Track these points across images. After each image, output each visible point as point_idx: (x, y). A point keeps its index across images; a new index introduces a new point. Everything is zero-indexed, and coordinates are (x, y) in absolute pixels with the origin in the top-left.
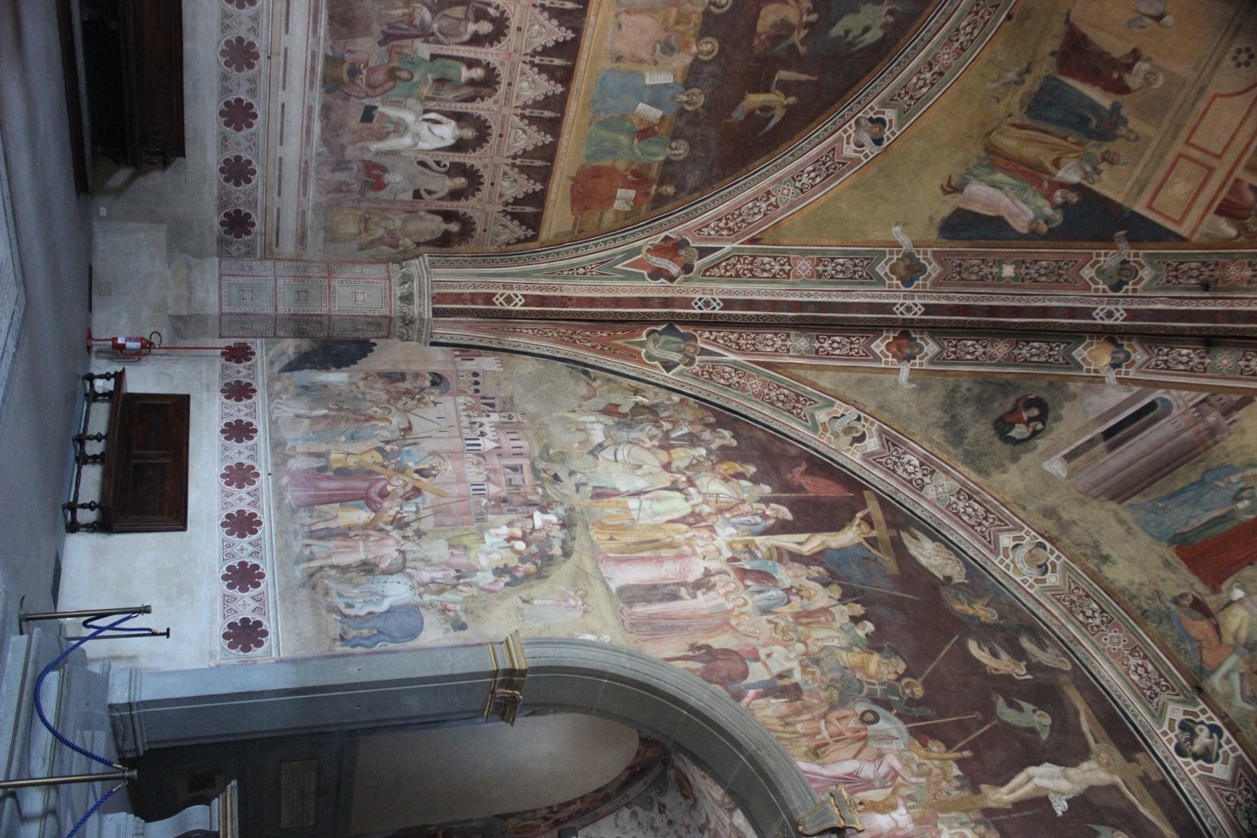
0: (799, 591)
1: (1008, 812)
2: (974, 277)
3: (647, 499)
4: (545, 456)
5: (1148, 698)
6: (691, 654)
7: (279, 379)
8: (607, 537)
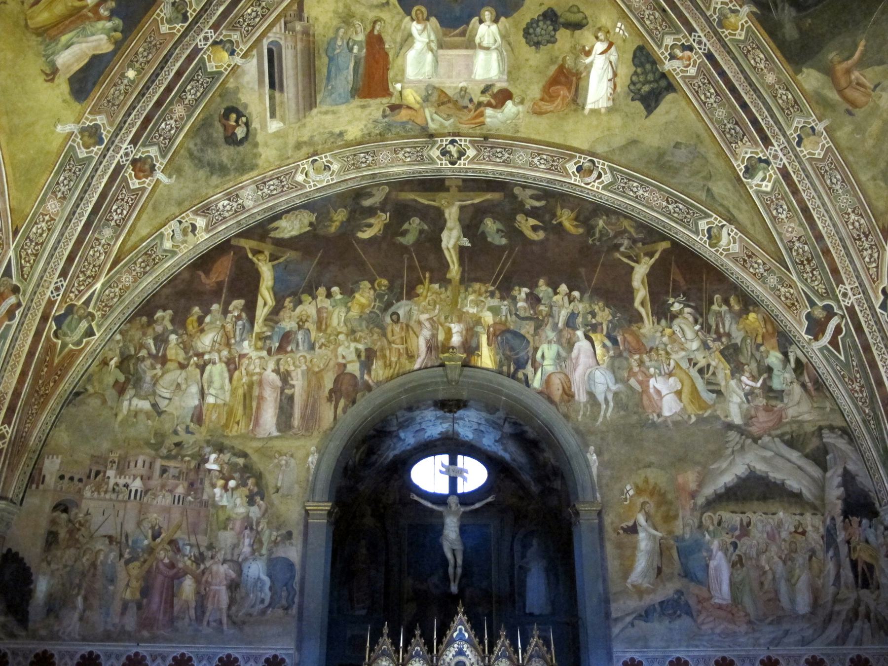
0: (301, 320)
1: (463, 272)
2: (122, 98)
5: (421, 160)
8: (236, 426)
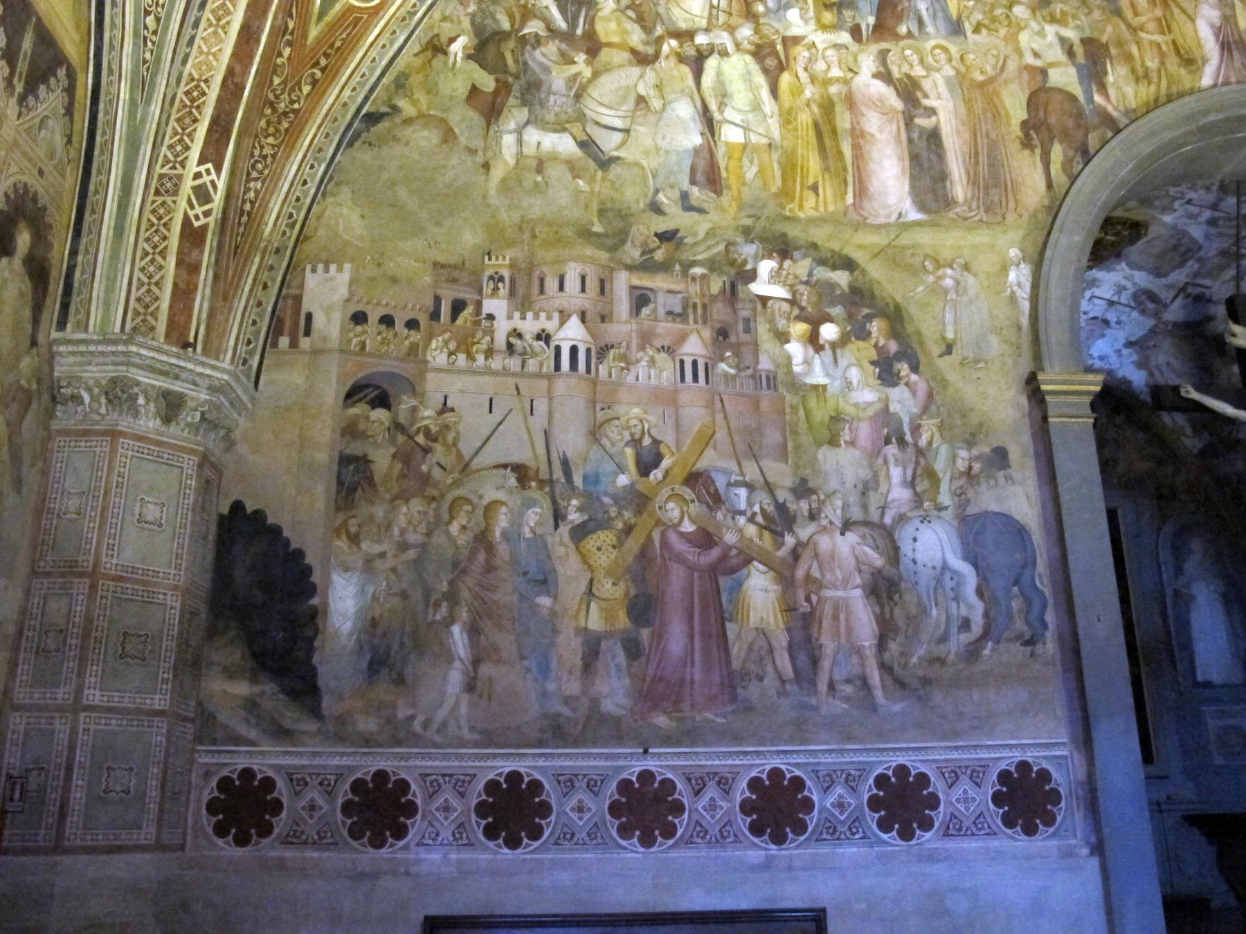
3: (721, 110)
6: (1038, 151)
7: (341, 720)
8: (810, 196)
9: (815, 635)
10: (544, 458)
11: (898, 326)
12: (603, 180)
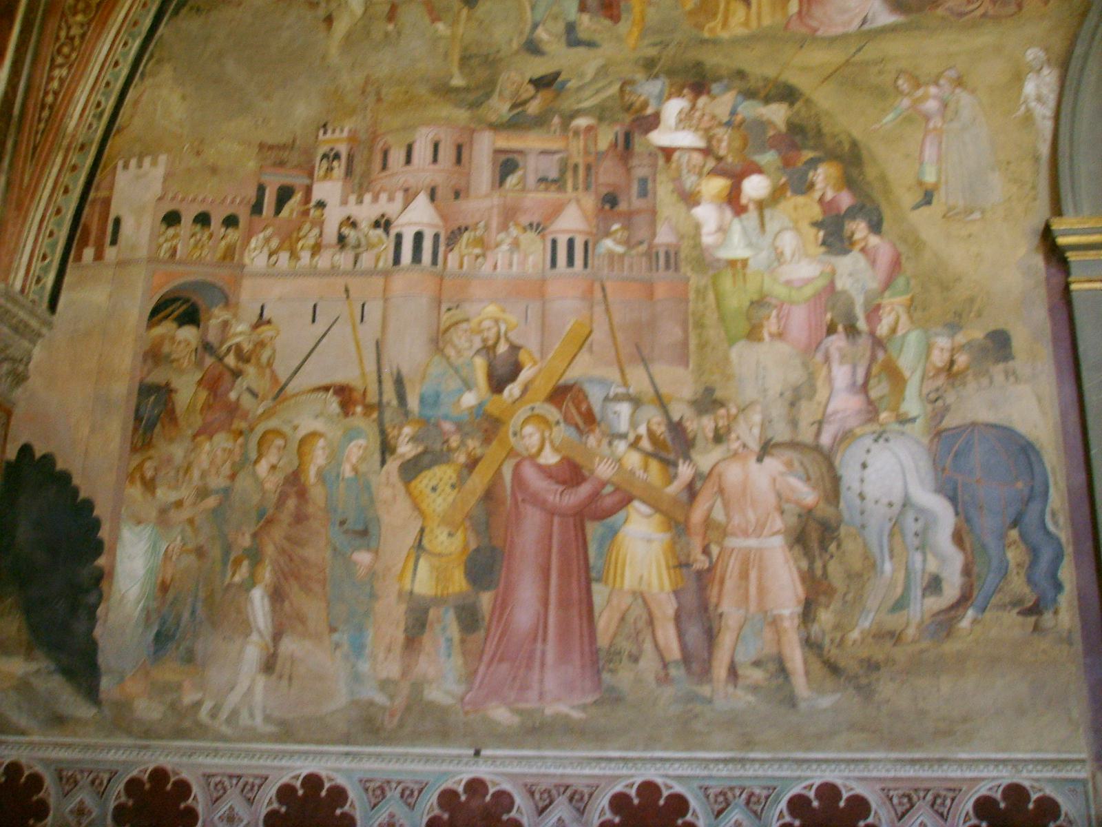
4: (471, 97)
9: (714, 600)
10: (373, 377)
11: (854, 172)
12: (469, 19)
